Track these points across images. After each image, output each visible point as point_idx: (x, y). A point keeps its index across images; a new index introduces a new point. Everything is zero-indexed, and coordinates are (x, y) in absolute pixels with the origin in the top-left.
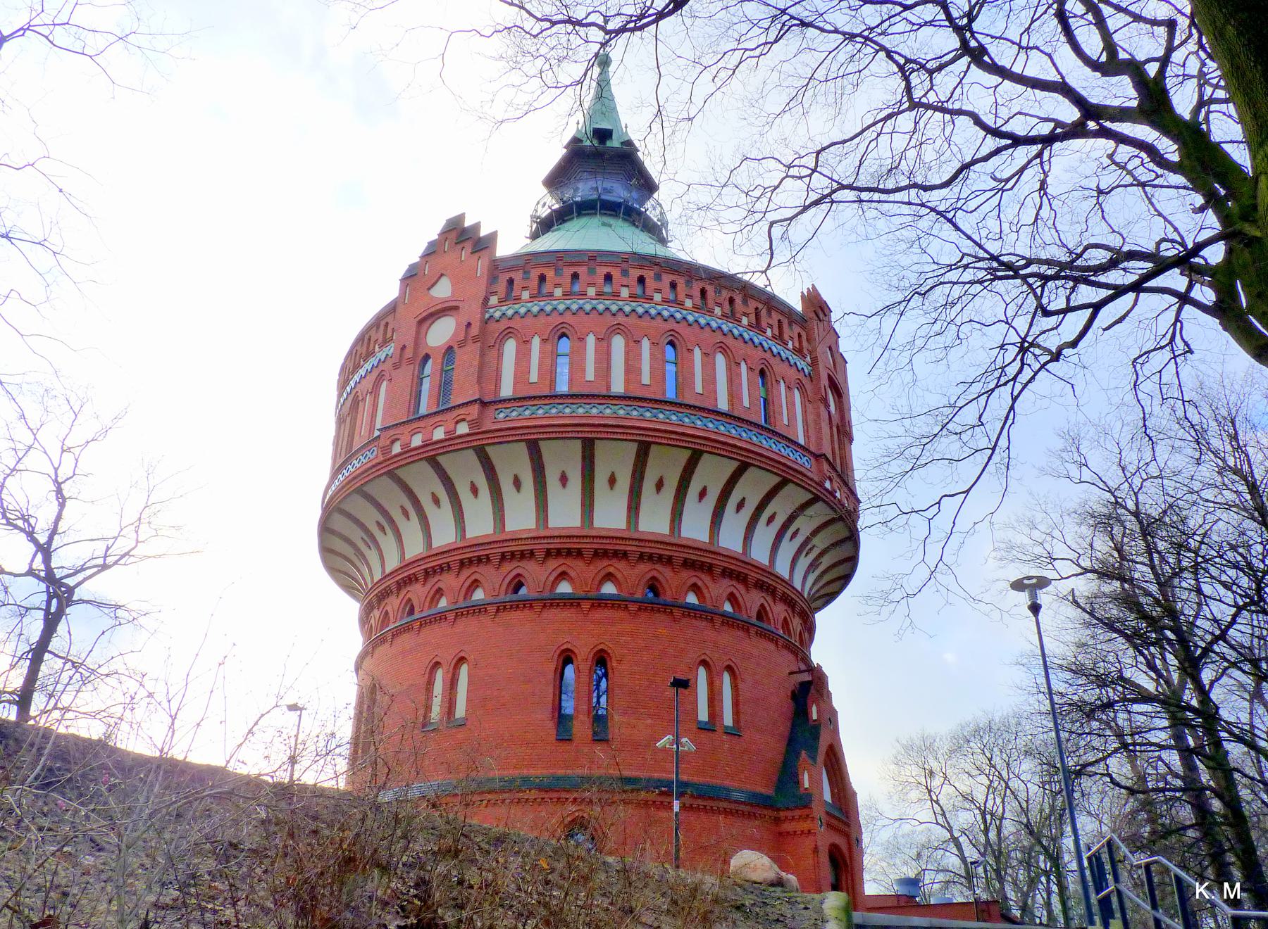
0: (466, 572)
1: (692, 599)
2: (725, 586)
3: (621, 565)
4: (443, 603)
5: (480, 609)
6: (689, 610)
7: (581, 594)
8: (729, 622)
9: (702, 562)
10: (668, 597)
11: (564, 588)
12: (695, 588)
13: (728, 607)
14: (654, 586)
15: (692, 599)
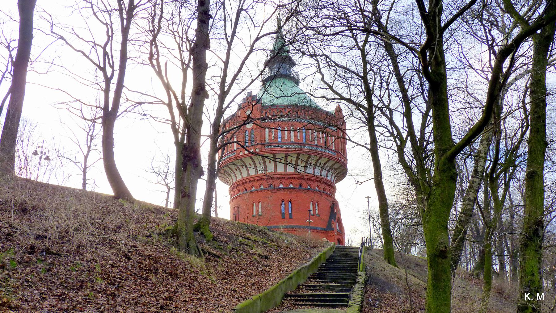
0: (259, 182)
1: (309, 187)
2: (317, 183)
3: (294, 180)
4: (254, 188)
5: (262, 190)
6: (308, 190)
7: (285, 187)
8: (317, 192)
9: (312, 179)
10: (304, 187)
11: (281, 186)
12: (310, 185)
13: (317, 189)
14: (301, 185)
15: (309, 187)
